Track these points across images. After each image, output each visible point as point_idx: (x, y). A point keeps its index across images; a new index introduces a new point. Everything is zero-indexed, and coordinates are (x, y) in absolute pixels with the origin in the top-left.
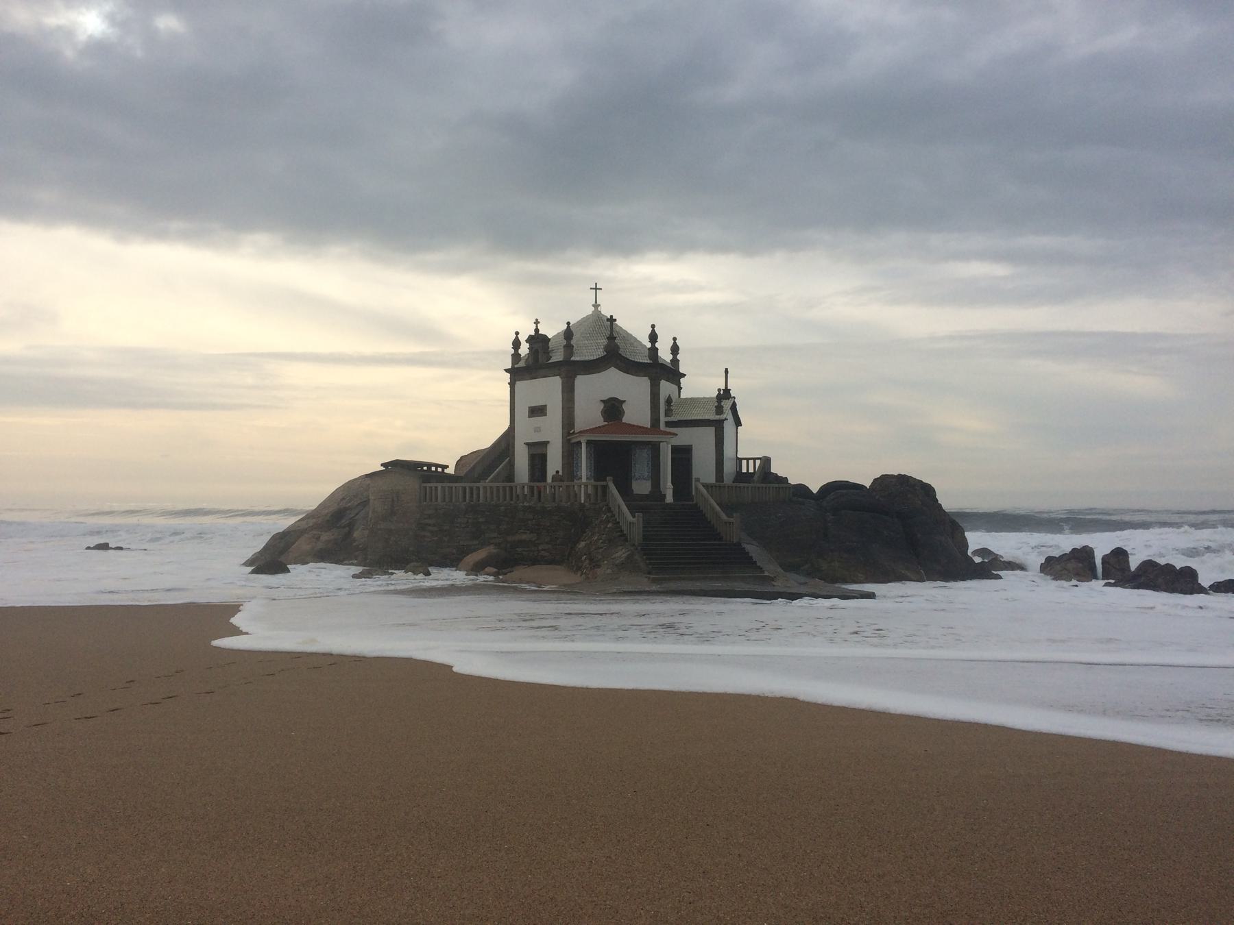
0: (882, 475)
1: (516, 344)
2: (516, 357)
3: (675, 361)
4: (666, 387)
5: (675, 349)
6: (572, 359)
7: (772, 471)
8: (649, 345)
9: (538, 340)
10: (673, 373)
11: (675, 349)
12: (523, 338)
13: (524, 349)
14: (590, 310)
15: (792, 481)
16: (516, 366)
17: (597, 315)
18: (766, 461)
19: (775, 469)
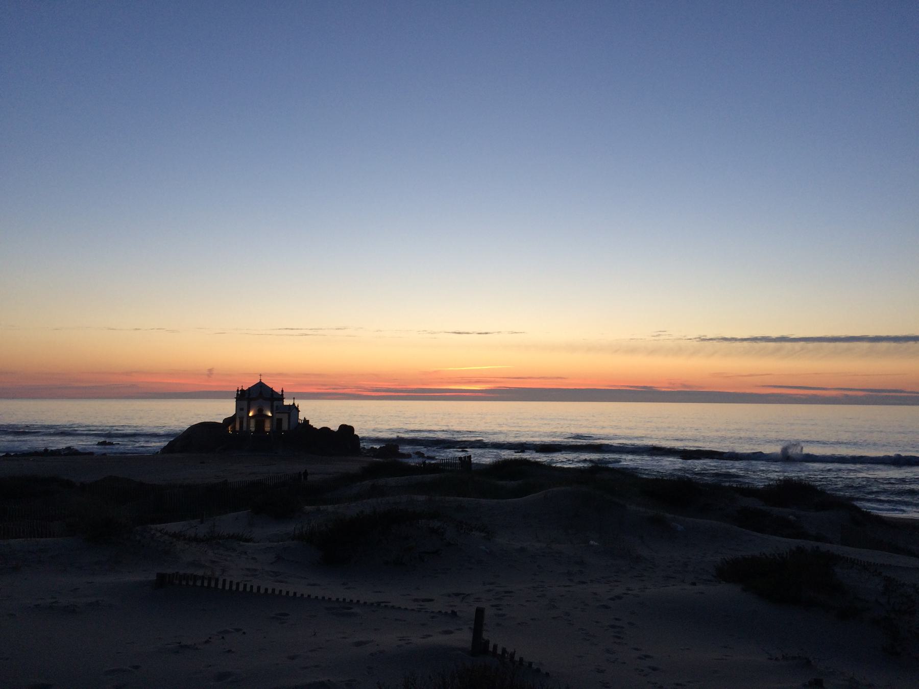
0: (342, 425)
1: (238, 390)
2: (237, 394)
3: (282, 395)
4: (276, 403)
5: (282, 391)
6: (251, 397)
7: (310, 424)
8: (271, 392)
9: (242, 390)
10: (281, 398)
11: (282, 391)
12: (240, 389)
13: (239, 393)
14: (259, 381)
15: (314, 427)
16: (238, 397)
17: (260, 382)
18: (308, 421)
19: (311, 423)
